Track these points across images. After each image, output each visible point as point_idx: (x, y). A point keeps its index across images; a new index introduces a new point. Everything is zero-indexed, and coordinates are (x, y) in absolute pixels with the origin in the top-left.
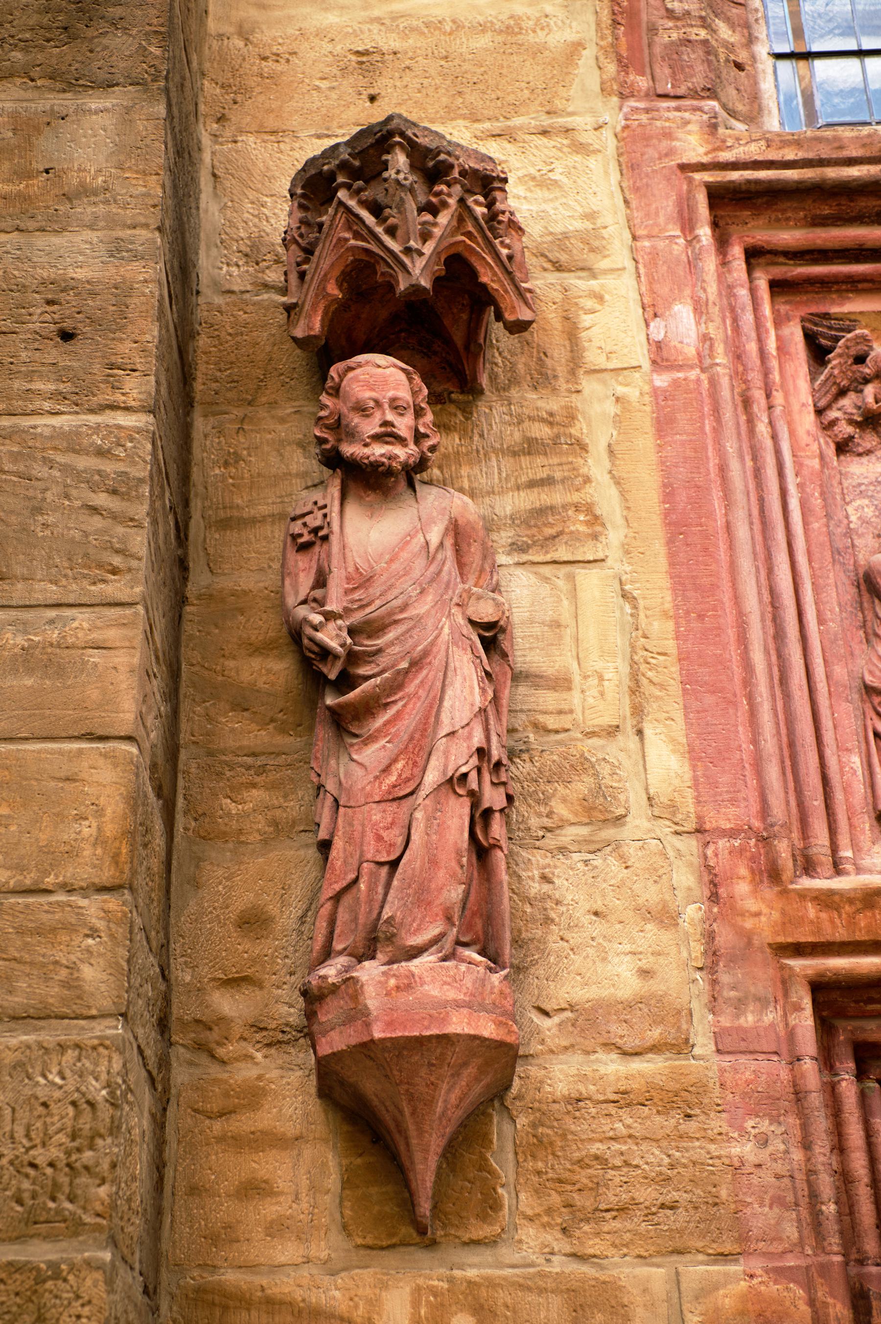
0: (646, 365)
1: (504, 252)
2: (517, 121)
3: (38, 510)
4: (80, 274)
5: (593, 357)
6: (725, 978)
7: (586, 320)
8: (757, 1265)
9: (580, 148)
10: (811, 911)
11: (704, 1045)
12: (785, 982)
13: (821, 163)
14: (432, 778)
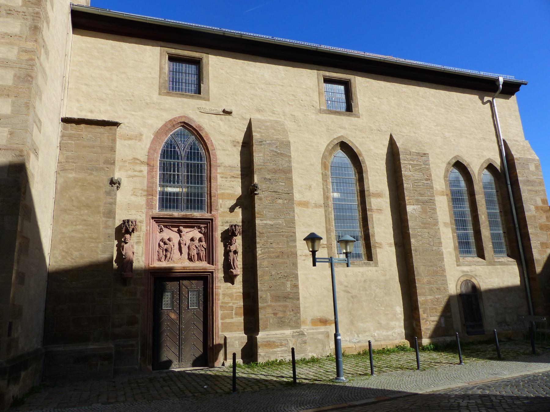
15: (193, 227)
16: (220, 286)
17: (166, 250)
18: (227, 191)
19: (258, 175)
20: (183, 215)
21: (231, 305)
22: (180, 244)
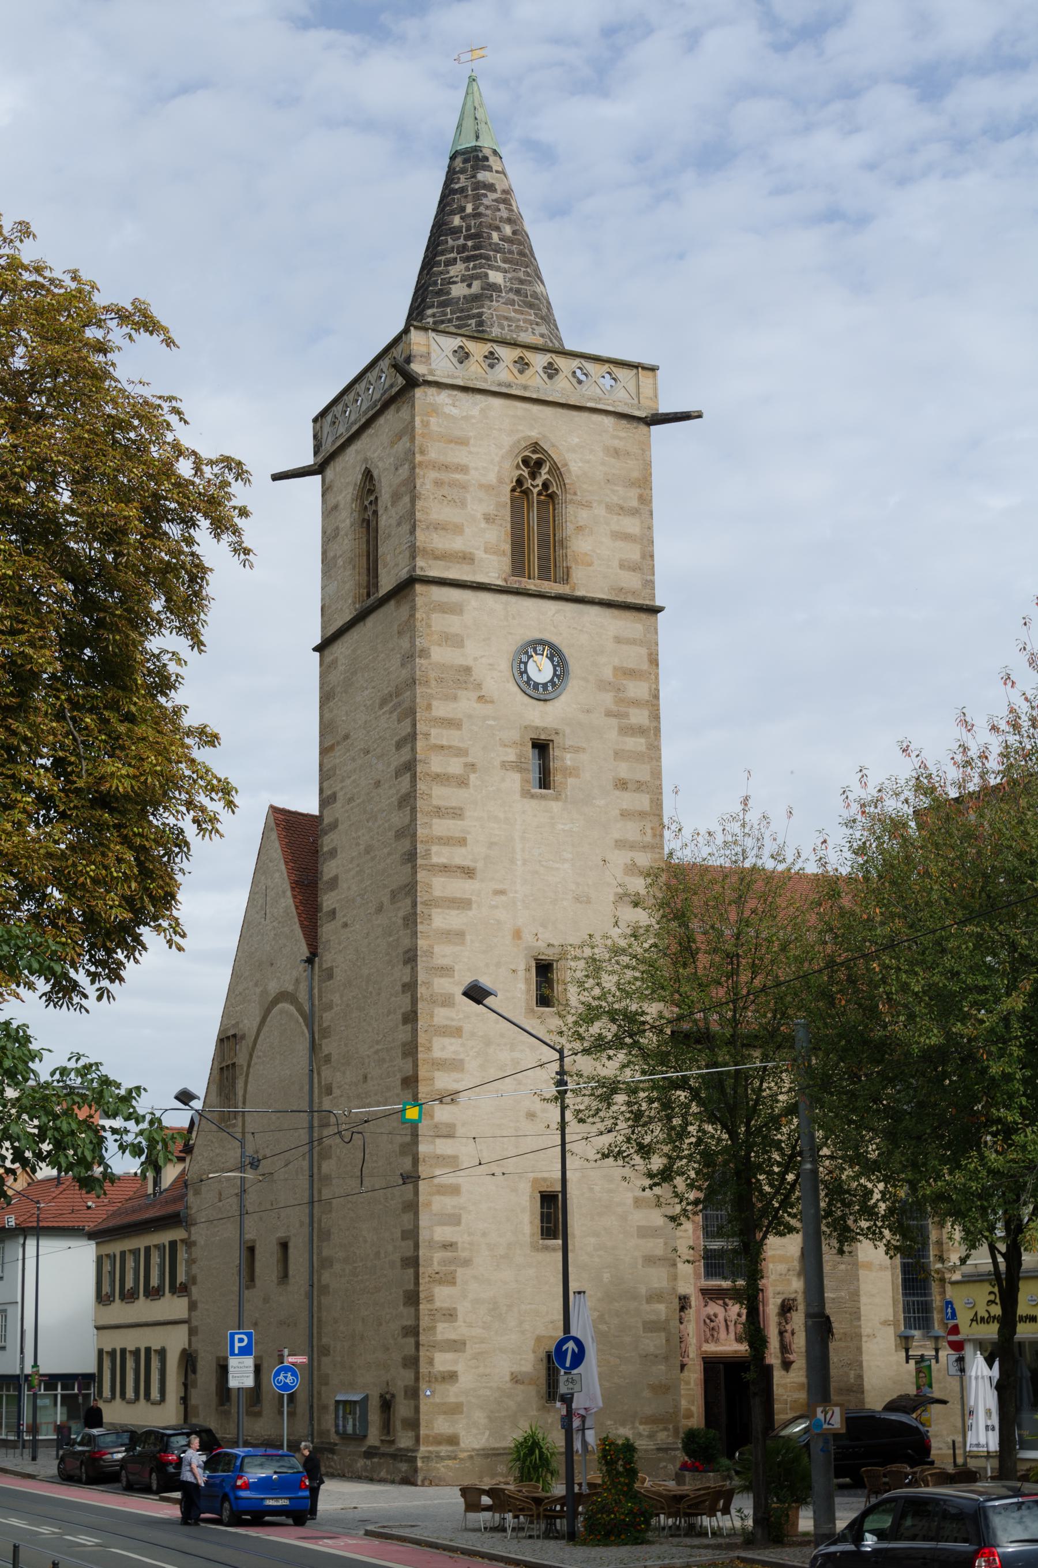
17: (713, 1329)
18: (778, 1252)
22: (726, 1321)
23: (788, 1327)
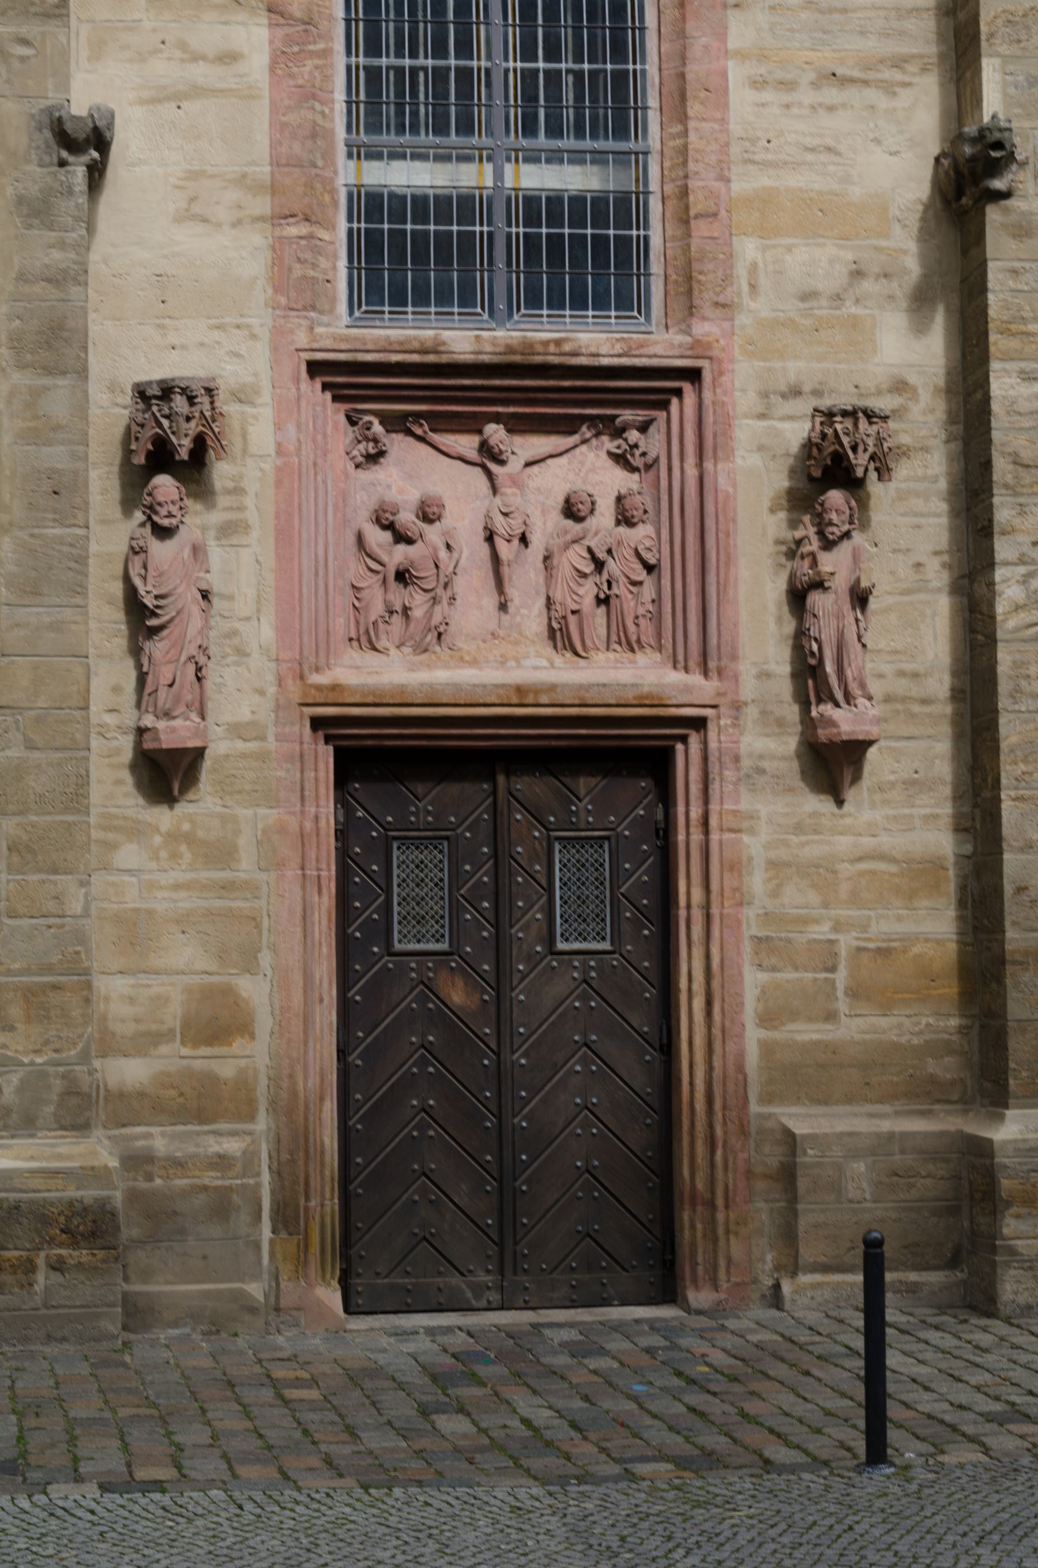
0: (272, 452)
1: (216, 430)
2: (227, 320)
3: (50, 568)
4: (59, 466)
5: (253, 449)
6: (281, 715)
7: (251, 429)
8: (281, 811)
9: (254, 337)
10: (313, 691)
11: (271, 738)
12: (302, 716)
13: (356, 351)
14: (183, 658)
15: (566, 426)
16: (752, 816)
18: (794, 180)
19: (1005, 59)
20: (510, 350)
21: (822, 931)
23: (835, 564)
